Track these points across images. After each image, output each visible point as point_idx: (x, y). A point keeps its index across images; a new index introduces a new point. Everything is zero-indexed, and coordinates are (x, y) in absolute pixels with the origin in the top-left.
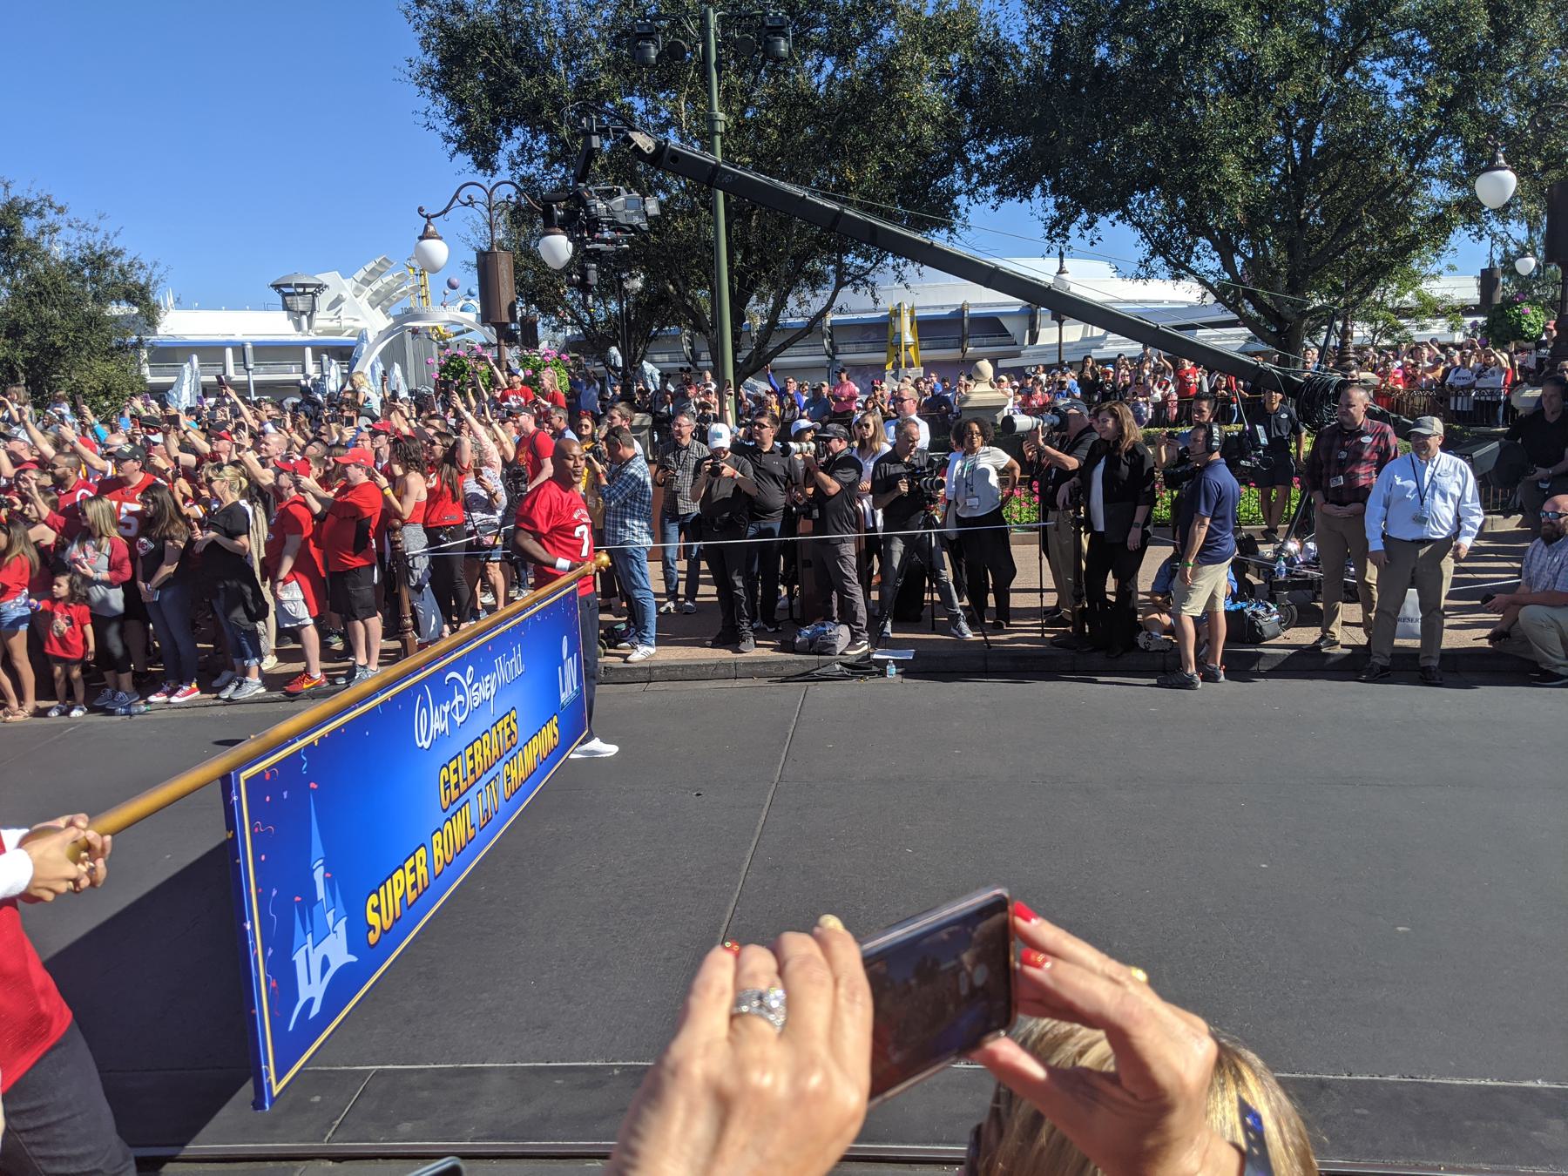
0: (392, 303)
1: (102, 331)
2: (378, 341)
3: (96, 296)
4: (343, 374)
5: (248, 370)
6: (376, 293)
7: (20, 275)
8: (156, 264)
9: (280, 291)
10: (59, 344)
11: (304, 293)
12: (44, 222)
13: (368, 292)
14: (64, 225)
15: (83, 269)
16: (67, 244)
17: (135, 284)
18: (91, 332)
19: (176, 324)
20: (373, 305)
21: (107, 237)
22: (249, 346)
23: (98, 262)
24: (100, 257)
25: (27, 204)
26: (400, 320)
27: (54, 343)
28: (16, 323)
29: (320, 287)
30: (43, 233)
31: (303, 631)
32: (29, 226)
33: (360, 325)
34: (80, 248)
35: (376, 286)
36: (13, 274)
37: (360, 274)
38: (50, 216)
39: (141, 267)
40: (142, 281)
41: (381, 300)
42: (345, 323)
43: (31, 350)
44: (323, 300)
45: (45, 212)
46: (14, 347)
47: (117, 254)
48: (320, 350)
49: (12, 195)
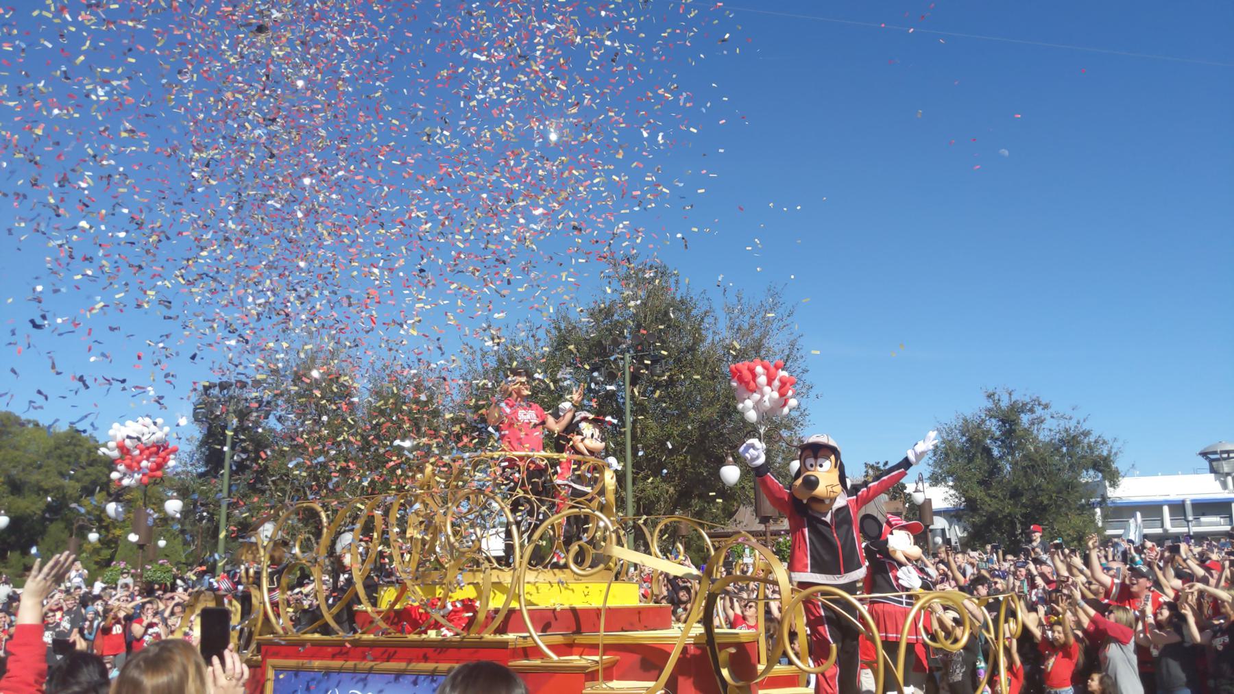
3: (1071, 466)
5: (1188, 521)
7: (1018, 455)
8: (1115, 439)
9: (1207, 458)
10: (1046, 502)
11: (1229, 458)
12: (1034, 416)
14: (1048, 417)
17: (1099, 456)
19: (1129, 489)
21: (1078, 423)
22: (1188, 502)
23: (1072, 441)
27: (1042, 502)
28: (1016, 488)
30: (1033, 424)
32: (1025, 419)
36: (1013, 455)
38: (1039, 411)
39: (1105, 443)
40: (1105, 453)
46: (1015, 505)
47: (1086, 434)
49: (1013, 400)
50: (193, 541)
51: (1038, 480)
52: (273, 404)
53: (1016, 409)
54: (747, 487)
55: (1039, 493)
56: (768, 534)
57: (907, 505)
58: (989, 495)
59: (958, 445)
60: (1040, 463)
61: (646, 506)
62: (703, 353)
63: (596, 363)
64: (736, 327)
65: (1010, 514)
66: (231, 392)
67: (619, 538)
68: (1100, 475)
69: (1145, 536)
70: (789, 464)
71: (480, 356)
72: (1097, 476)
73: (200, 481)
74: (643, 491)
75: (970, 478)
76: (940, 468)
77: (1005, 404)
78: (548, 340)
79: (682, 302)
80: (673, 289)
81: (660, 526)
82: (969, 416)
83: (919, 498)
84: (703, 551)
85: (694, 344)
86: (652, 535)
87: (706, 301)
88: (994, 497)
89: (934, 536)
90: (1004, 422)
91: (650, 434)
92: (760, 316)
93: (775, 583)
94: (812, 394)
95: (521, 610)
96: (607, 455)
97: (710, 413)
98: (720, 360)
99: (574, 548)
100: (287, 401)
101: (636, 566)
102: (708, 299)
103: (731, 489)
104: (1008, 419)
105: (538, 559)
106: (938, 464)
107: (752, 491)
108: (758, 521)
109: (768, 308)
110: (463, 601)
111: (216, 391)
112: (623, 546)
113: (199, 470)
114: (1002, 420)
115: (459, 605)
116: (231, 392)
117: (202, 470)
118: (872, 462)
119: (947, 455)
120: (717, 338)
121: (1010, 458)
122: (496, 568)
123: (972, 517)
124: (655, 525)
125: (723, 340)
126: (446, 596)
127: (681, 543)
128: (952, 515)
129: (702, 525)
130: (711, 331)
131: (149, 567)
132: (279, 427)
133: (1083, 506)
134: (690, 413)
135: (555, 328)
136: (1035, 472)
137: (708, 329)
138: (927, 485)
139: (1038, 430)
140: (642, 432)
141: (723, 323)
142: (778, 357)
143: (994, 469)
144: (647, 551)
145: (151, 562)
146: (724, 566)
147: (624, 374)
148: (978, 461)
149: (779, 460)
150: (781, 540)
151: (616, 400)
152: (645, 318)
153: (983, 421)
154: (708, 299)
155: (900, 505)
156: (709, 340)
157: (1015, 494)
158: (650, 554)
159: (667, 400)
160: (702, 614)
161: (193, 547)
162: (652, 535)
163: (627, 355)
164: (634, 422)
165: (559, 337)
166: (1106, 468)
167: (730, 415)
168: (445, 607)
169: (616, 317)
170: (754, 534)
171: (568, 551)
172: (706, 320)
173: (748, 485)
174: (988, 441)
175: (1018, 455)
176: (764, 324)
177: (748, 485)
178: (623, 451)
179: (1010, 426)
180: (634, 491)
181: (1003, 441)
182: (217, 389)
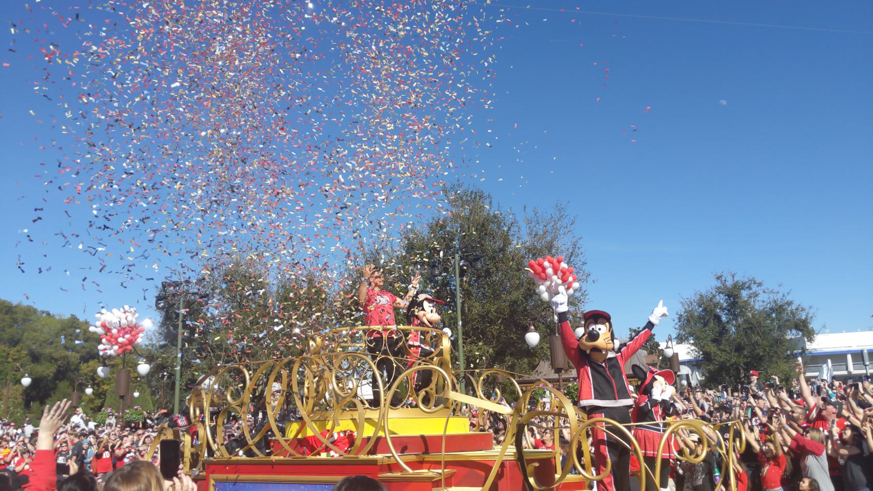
1: (784, 346)
5: (866, 366)
7: (740, 320)
8: (811, 307)
10: (761, 354)
12: (751, 291)
14: (761, 292)
15: (772, 313)
16: (763, 302)
17: (800, 320)
18: (778, 346)
19: (822, 343)
22: (865, 352)
23: (779, 309)
24: (781, 306)
28: (739, 344)
30: (751, 297)
32: (744, 294)
34: (770, 303)
36: (736, 320)
38: (754, 288)
39: (803, 310)
40: (803, 317)
45: (752, 286)
46: (739, 356)
47: (790, 304)
49: (736, 280)
50: (158, 393)
51: (756, 338)
54: (545, 347)
55: (757, 347)
56: (561, 381)
57: (660, 358)
58: (720, 349)
59: (696, 314)
60: (756, 325)
62: (510, 252)
64: (534, 233)
65: (735, 363)
66: (181, 288)
68: (800, 333)
69: (834, 378)
72: (798, 334)
75: (706, 338)
77: (729, 283)
83: (669, 353)
85: (504, 246)
88: (723, 351)
89: (681, 380)
91: (475, 311)
92: (551, 225)
93: (566, 416)
94: (590, 279)
95: (385, 438)
96: (444, 327)
97: (516, 295)
98: (523, 257)
99: (422, 393)
101: (466, 405)
102: (513, 214)
103: (533, 349)
104: (733, 294)
105: (396, 402)
106: (682, 327)
107: (549, 350)
108: (553, 371)
109: (556, 219)
112: (457, 391)
114: (728, 295)
115: (342, 435)
119: (688, 321)
121: (734, 322)
122: (368, 408)
123: (708, 365)
124: (480, 375)
125: (525, 243)
126: (333, 428)
127: (499, 389)
128: (693, 364)
129: (513, 376)
130: (516, 237)
131: (128, 411)
133: (788, 356)
135: (405, 238)
136: (753, 332)
137: (514, 235)
138: (674, 343)
139: (754, 302)
140: (469, 309)
141: (524, 231)
142: (564, 254)
143: (723, 331)
144: (475, 395)
145: (129, 407)
146: (529, 404)
147: (455, 268)
148: (711, 325)
150: (570, 385)
153: (714, 296)
157: (739, 349)
158: (476, 397)
159: (486, 286)
160: (514, 439)
161: (158, 397)
162: (477, 383)
163: (457, 256)
164: (463, 303)
166: (805, 329)
167: (531, 296)
168: (332, 436)
169: (448, 229)
170: (550, 381)
171: (418, 395)
172: (512, 229)
173: (546, 346)
174: (718, 311)
176: (554, 231)
177: (546, 346)
178: (456, 323)
179: (734, 299)
180: (464, 352)
181: (728, 310)
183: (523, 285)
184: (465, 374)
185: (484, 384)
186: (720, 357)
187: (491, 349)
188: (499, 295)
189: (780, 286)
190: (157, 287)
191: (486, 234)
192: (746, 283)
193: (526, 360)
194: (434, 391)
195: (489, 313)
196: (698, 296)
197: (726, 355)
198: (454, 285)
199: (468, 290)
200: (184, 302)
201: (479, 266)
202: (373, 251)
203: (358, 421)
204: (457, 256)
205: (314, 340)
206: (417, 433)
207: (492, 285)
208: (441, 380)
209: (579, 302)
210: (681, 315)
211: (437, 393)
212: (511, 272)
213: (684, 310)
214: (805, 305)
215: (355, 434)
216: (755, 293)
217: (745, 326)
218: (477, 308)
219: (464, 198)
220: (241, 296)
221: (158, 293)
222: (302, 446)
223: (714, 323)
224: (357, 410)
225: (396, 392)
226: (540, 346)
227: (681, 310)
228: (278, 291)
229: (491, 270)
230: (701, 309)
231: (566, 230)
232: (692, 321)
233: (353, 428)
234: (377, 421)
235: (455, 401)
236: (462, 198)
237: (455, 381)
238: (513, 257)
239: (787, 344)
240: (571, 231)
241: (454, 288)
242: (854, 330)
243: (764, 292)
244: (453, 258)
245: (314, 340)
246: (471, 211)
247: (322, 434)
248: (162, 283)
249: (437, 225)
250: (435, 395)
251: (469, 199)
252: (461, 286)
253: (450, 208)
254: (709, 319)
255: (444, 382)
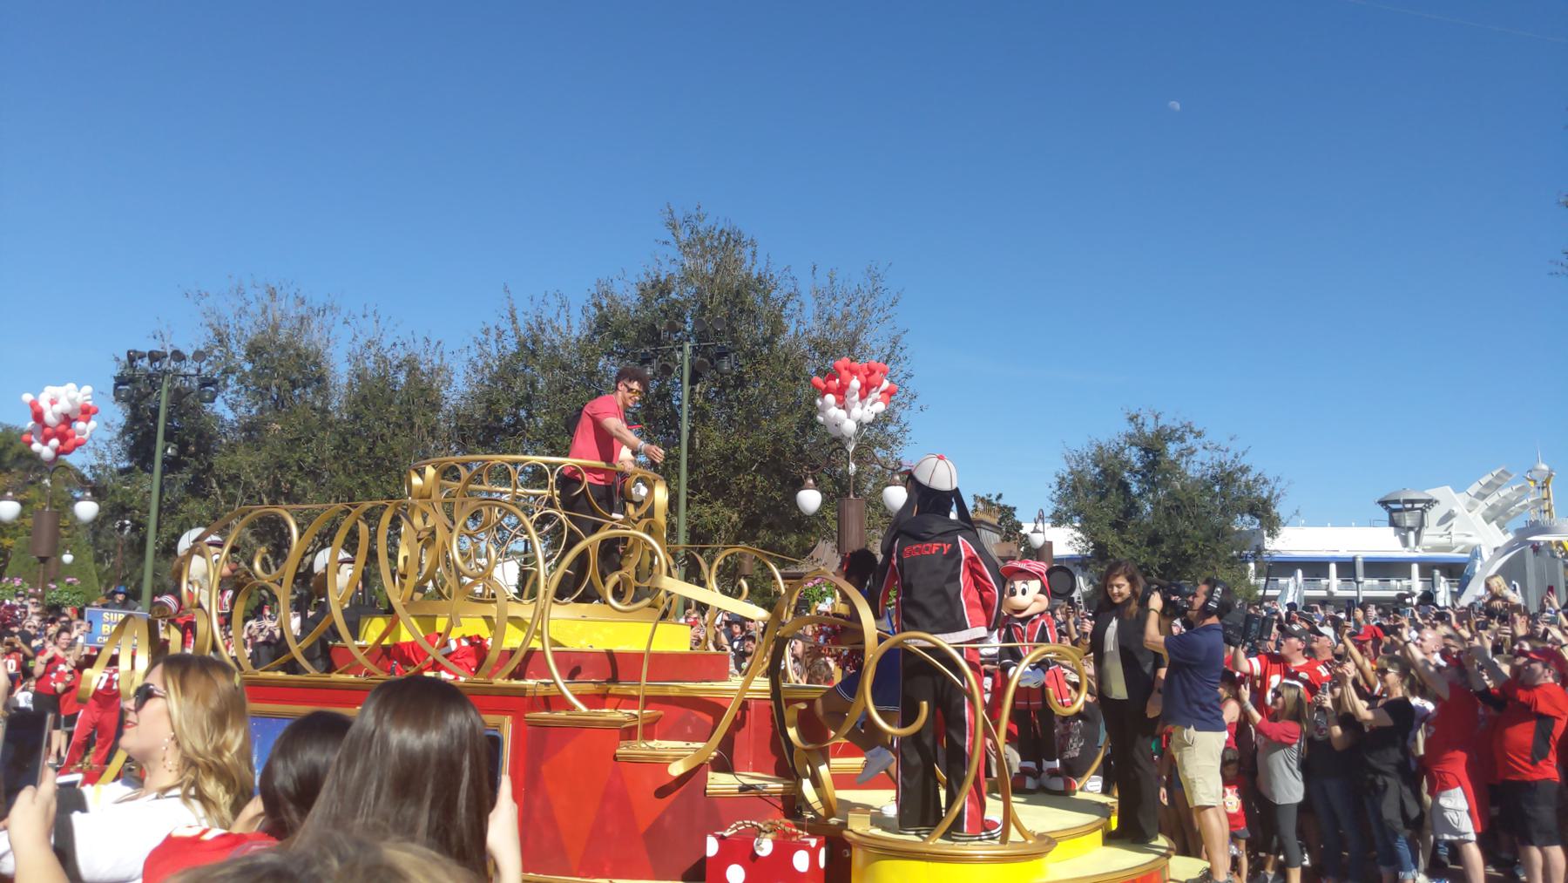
0: (1509, 517)
1: (1228, 540)
2: (1493, 560)
4: (1452, 592)
6: (1492, 507)
7: (1161, 493)
10: (1190, 552)
11: (1413, 509)
12: (1183, 446)
13: (1483, 506)
14: (1200, 448)
15: (1214, 485)
16: (1202, 464)
17: (1258, 498)
19: (1290, 541)
20: (1488, 520)
21: (1236, 457)
22: (1360, 560)
23: (1226, 478)
24: (1229, 474)
25: (1172, 431)
26: (1522, 535)
28: (1155, 533)
29: (1430, 503)
30: (1182, 455)
31: (1464, 846)
32: (1172, 449)
33: (1473, 541)
34: (1213, 467)
35: (1491, 500)
36: (1155, 493)
37: (1475, 488)
38: (1190, 440)
39: (1265, 482)
40: (1265, 495)
41: (1497, 515)
42: (1455, 539)
43: (1167, 557)
44: (1433, 515)
46: (1154, 553)
47: (1244, 470)
48: (1427, 568)
49: (1160, 424)
51: (1182, 524)
52: (221, 383)
53: (1163, 436)
55: (1183, 540)
57: (1022, 549)
59: (1088, 478)
60: (1186, 503)
61: (700, 536)
62: (782, 346)
63: (646, 353)
64: (826, 316)
65: (1145, 565)
67: (669, 570)
68: (1258, 521)
70: (881, 491)
71: (495, 337)
73: (122, 478)
74: (699, 516)
75: (1101, 519)
76: (1066, 504)
77: (1149, 429)
78: (584, 320)
79: (760, 280)
80: (749, 263)
81: (719, 561)
82: (1104, 440)
83: (1038, 540)
84: (769, 595)
86: (710, 569)
87: (790, 282)
90: (1147, 451)
91: (712, 447)
92: (856, 304)
94: (916, 405)
95: (543, 652)
97: (788, 423)
98: (804, 357)
99: (614, 578)
100: (240, 381)
102: (793, 278)
103: (808, 517)
104: (1152, 448)
105: (561, 594)
106: (1062, 500)
109: (866, 293)
110: (469, 639)
111: (145, 363)
113: (121, 465)
115: (465, 643)
116: (165, 366)
117: (126, 464)
118: (982, 494)
119: (1075, 489)
120: (802, 329)
121: (1151, 496)
126: (449, 630)
130: (794, 320)
132: (229, 416)
133: (1233, 558)
134: (764, 422)
135: (595, 305)
136: (1180, 514)
138: (1048, 525)
139: (1187, 463)
140: (701, 443)
141: (810, 310)
142: (876, 357)
143: (1131, 509)
144: (702, 584)
148: (1113, 498)
149: (870, 486)
151: (670, 401)
152: (712, 297)
153: (1122, 449)
154: (793, 278)
155: (1014, 548)
156: (792, 331)
157: (1154, 541)
159: (736, 404)
162: (710, 569)
163: (687, 346)
164: (692, 431)
165: (601, 316)
166: (1265, 514)
167: (813, 427)
168: (446, 644)
169: (673, 295)
172: (789, 305)
174: (1126, 474)
175: (1161, 493)
179: (1155, 456)
181: (1143, 475)
182: (147, 360)
183: (799, 407)
184: (686, 551)
185: (717, 576)
186: (1122, 552)
187: (736, 515)
188: (757, 421)
189: (1231, 439)
190: (117, 359)
191: (742, 311)
192: (1177, 430)
193: (794, 538)
194: (632, 577)
195: (735, 452)
196: (1095, 448)
197: (1132, 551)
198: (678, 399)
199: (703, 409)
200: (169, 390)
201: (726, 367)
202: (534, 325)
203: (495, 620)
204: (687, 346)
205: (421, 473)
206: (600, 647)
207: (749, 400)
208: (647, 559)
209: (893, 443)
210: (1063, 479)
211: (637, 579)
212: (781, 382)
213: (1069, 470)
214: (1269, 475)
215: (489, 643)
216: (1190, 448)
217: (1168, 504)
218: (717, 442)
219: (707, 243)
220: (279, 388)
221: (119, 371)
222: (390, 659)
223: (1118, 495)
224: (495, 602)
225: (565, 575)
226: (819, 515)
227: (1064, 469)
228: (350, 384)
229: (746, 376)
230: (1097, 470)
231: (882, 316)
232: (1080, 489)
233: (485, 633)
234: (529, 621)
235: (669, 594)
236: (702, 242)
237: (672, 563)
238: (786, 355)
239: (1233, 538)
240: (890, 317)
241: (677, 403)
242: (1346, 524)
243: (1205, 448)
244: (681, 349)
245: (421, 473)
246: (718, 266)
247: (427, 638)
248: (129, 352)
249: (653, 287)
250: (635, 583)
251: (716, 244)
252: (691, 400)
253: (680, 258)
254: (1111, 487)
255: (652, 563)
